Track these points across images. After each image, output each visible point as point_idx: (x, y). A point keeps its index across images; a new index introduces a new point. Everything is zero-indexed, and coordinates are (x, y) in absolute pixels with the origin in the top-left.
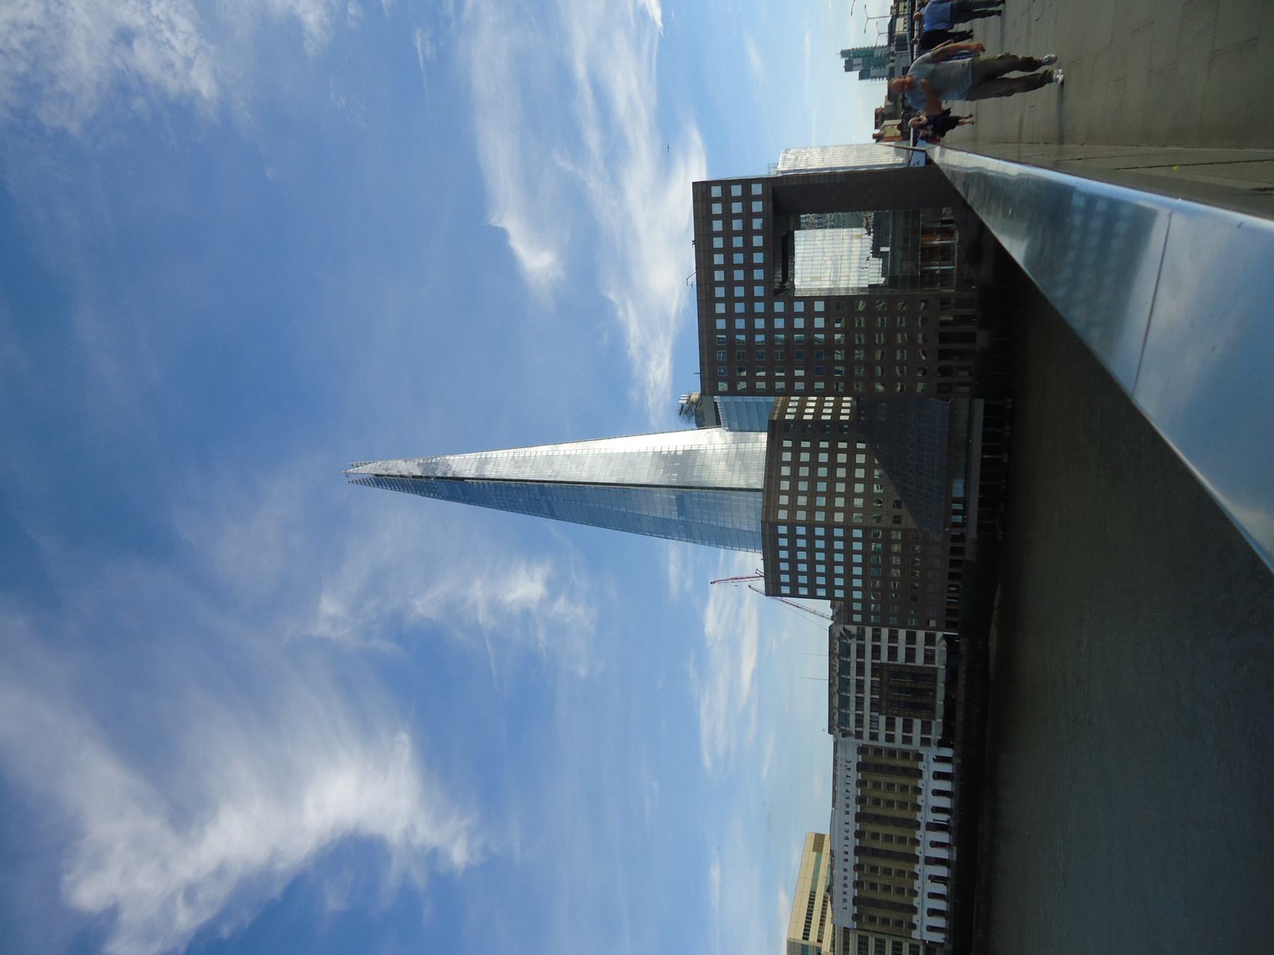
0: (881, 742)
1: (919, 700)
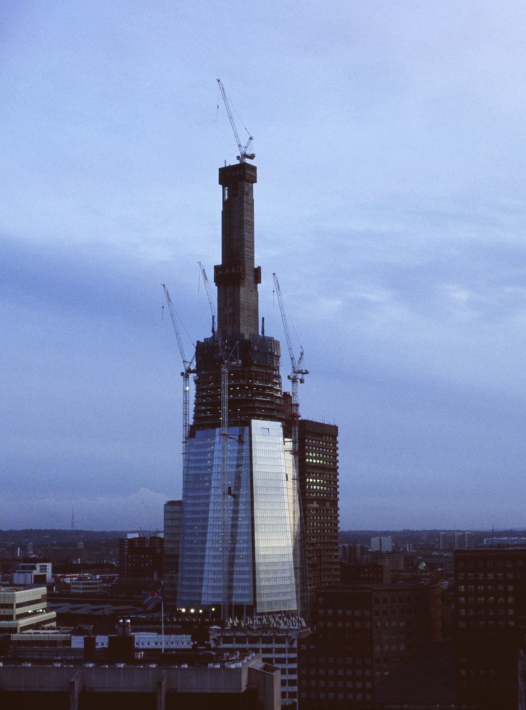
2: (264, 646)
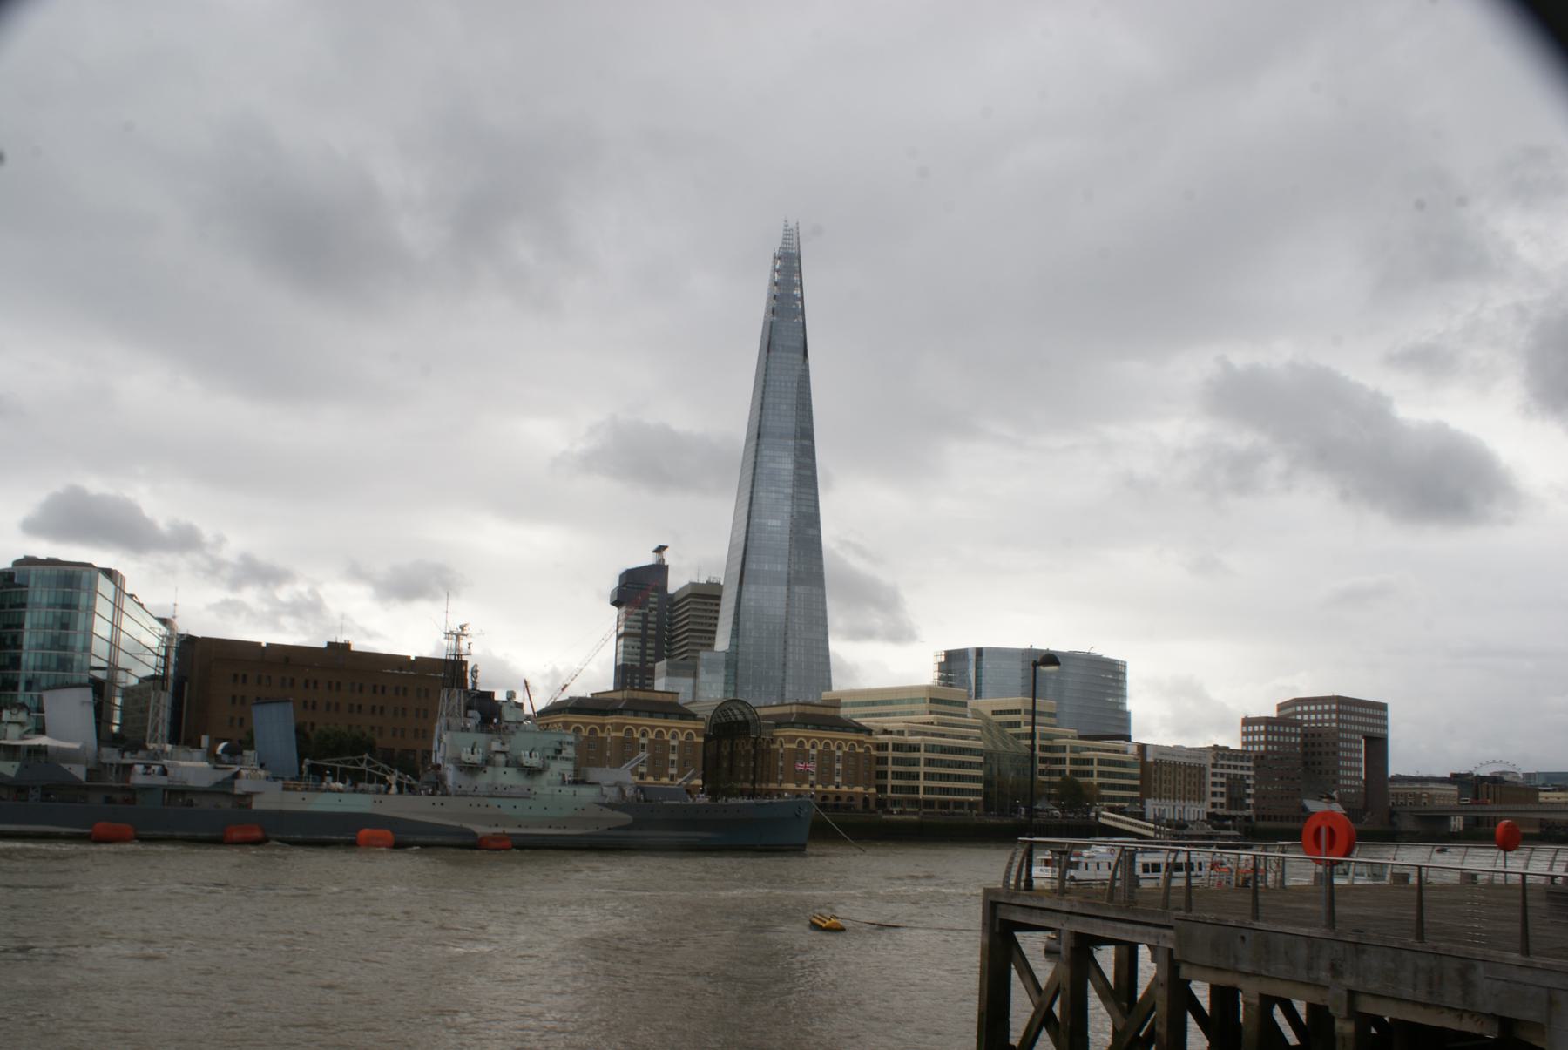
0: (1211, 779)
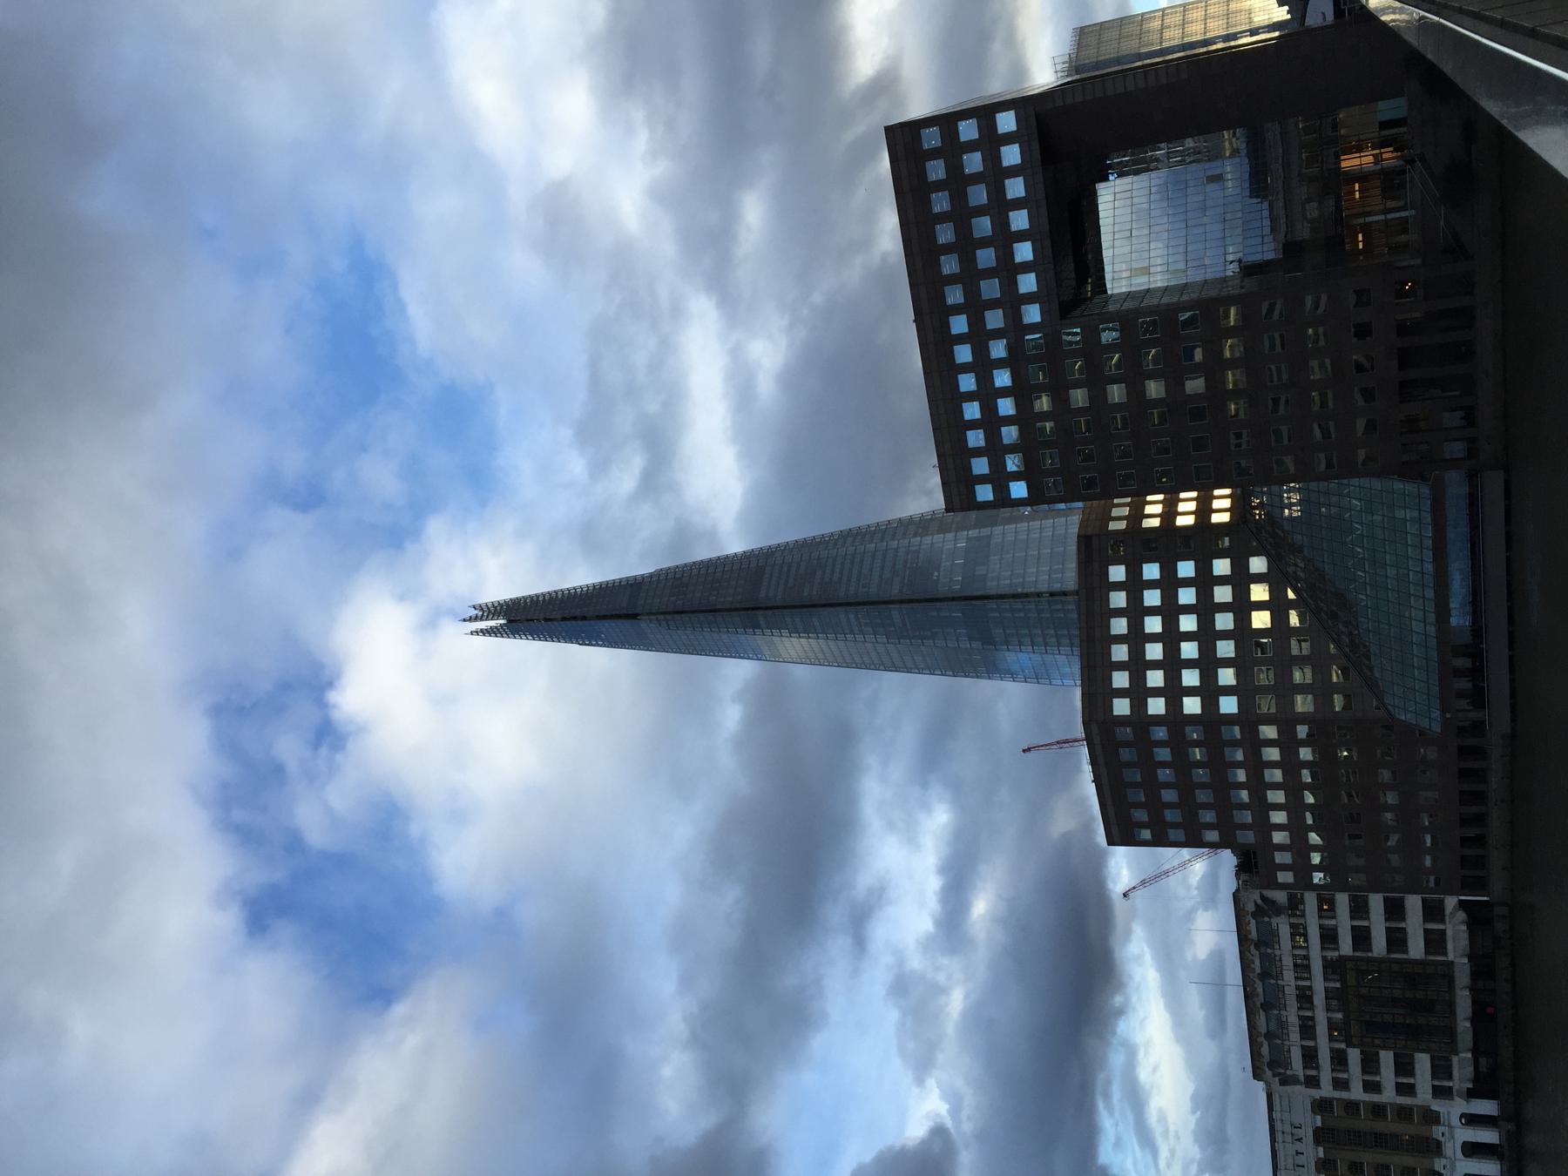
1: (1422, 1021)
2: (1289, 977)
